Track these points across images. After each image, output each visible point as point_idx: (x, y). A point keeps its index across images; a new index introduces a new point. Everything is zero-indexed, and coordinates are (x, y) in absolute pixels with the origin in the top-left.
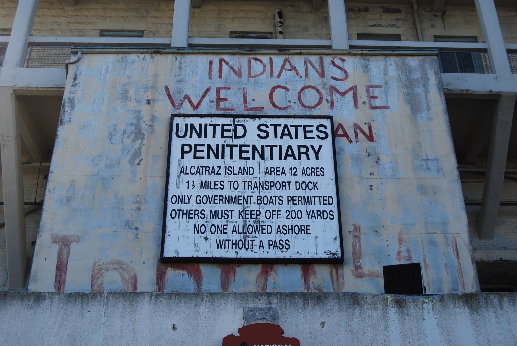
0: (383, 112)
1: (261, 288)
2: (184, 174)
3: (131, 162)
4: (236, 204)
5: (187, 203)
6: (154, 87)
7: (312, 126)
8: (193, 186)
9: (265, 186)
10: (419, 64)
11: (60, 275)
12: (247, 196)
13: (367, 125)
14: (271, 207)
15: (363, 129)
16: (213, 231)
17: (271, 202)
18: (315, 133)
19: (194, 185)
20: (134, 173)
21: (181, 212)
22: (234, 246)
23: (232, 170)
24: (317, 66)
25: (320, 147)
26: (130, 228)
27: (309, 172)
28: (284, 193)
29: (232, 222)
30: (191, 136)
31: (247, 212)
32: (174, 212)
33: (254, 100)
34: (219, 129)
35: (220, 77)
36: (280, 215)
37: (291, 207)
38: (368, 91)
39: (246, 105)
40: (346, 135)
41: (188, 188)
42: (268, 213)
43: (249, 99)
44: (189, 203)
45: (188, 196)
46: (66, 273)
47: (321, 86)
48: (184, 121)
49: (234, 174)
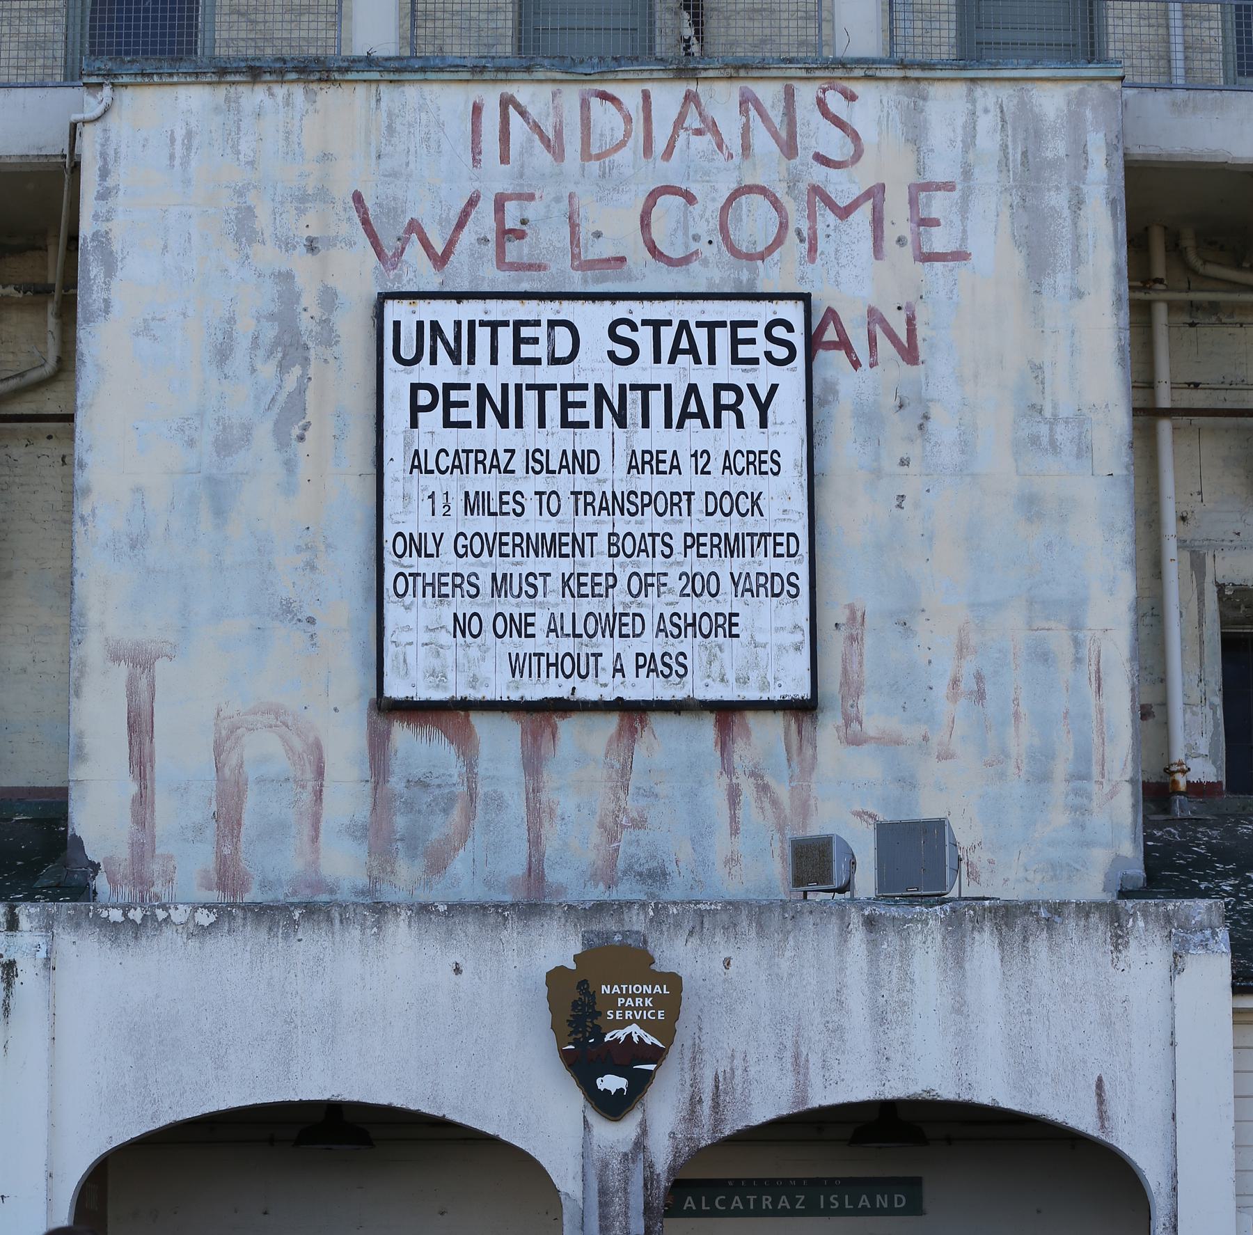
0: (950, 270)
1: (617, 771)
2: (421, 473)
4: (555, 556)
5: (432, 556)
6: (323, 194)
7: (753, 324)
8: (447, 508)
9: (627, 505)
10: (1065, 108)
11: (140, 743)
12: (583, 534)
13: (902, 311)
16: (500, 632)
17: (643, 551)
18: (763, 345)
19: (447, 505)
20: (290, 466)
21: (420, 579)
22: (553, 669)
23: (543, 459)
24: (776, 116)
25: (774, 388)
26: (296, 619)
27: (741, 462)
28: (678, 527)
30: (433, 361)
31: (583, 579)
32: (401, 579)
33: (598, 235)
34: (505, 335)
35: (505, 159)
36: (665, 585)
37: (693, 564)
38: (913, 202)
40: (844, 344)
41: (433, 514)
42: (635, 579)
43: (585, 232)
44: (438, 556)
45: (433, 534)
48: (414, 312)
49: (548, 472)
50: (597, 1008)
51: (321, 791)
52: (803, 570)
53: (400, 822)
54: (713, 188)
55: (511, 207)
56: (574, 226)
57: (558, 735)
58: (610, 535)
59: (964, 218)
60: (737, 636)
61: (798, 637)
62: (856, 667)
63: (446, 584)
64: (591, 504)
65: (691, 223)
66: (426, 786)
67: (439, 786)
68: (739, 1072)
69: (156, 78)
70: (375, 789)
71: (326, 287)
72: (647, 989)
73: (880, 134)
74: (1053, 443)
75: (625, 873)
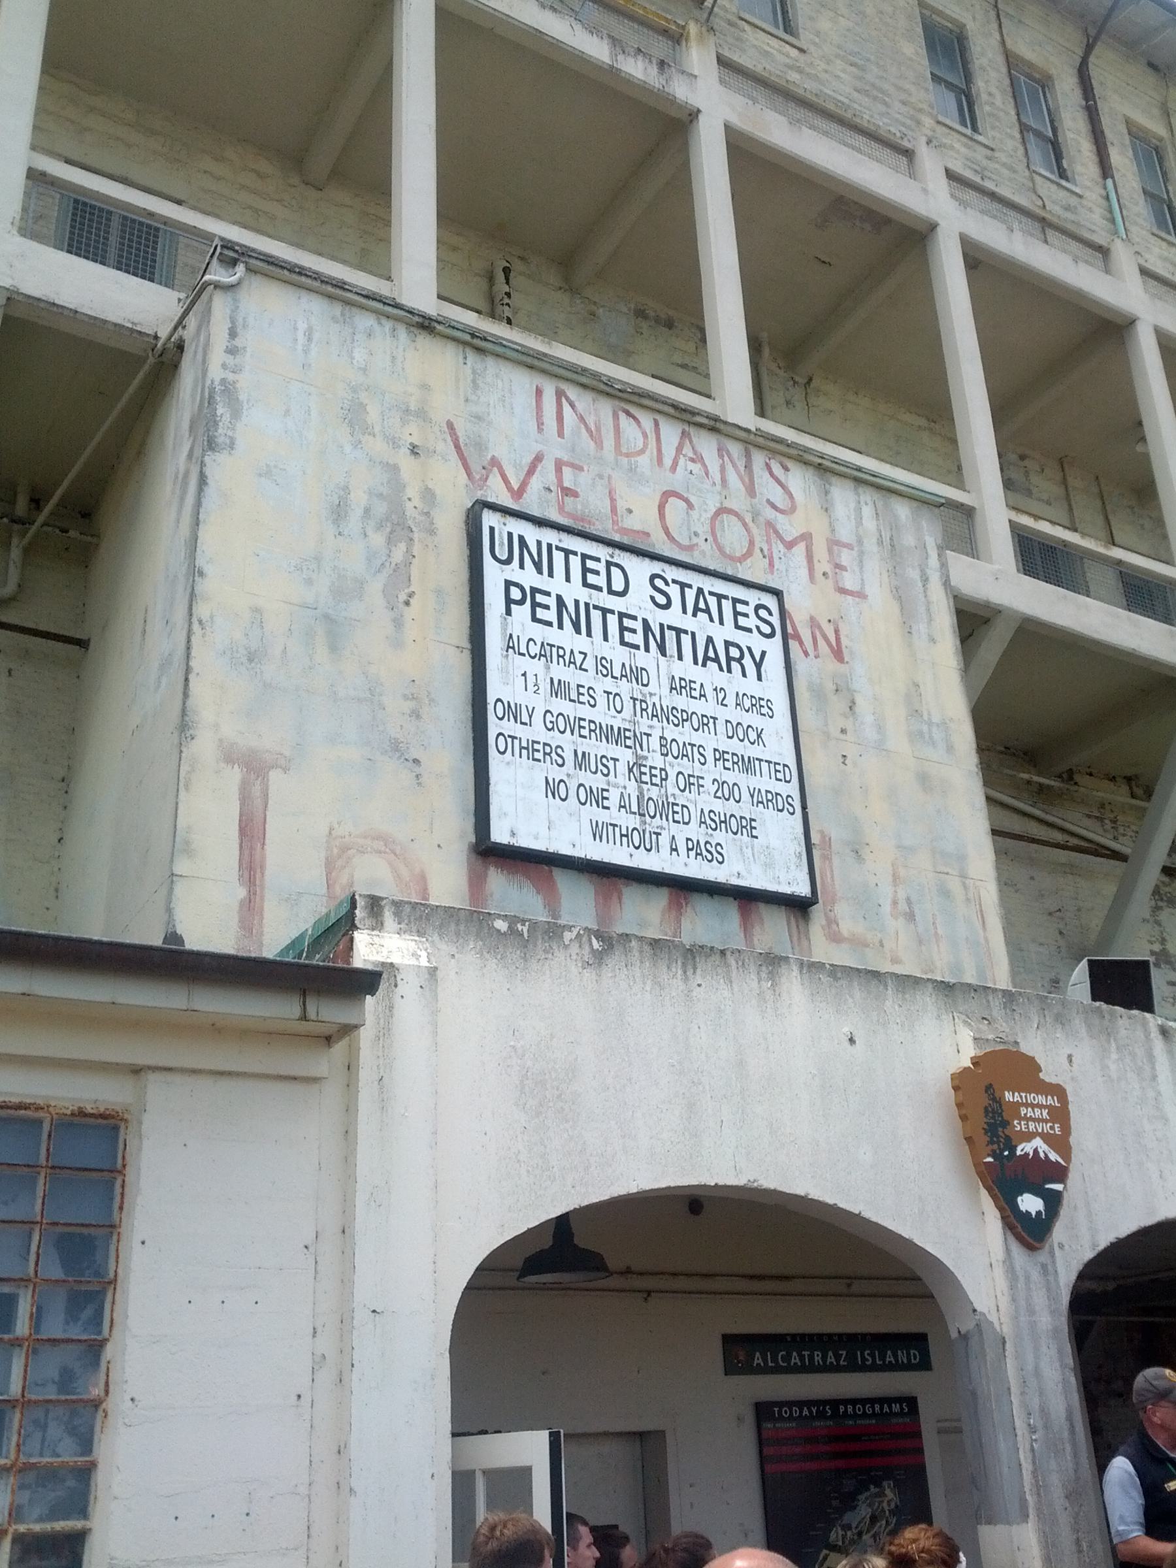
6: (422, 414)
9: (671, 717)
18: (752, 622)
20: (398, 623)
21: (516, 742)
23: (608, 666)
24: (741, 464)
25: (763, 654)
28: (710, 741)
29: (616, 786)
30: (522, 566)
31: (643, 769)
35: (561, 434)
38: (830, 551)
40: (797, 637)
46: (264, 844)
49: (612, 677)
52: (796, 795)
55: (567, 471)
63: (538, 751)
71: (427, 488)
72: (1041, 1099)
74: (931, 737)
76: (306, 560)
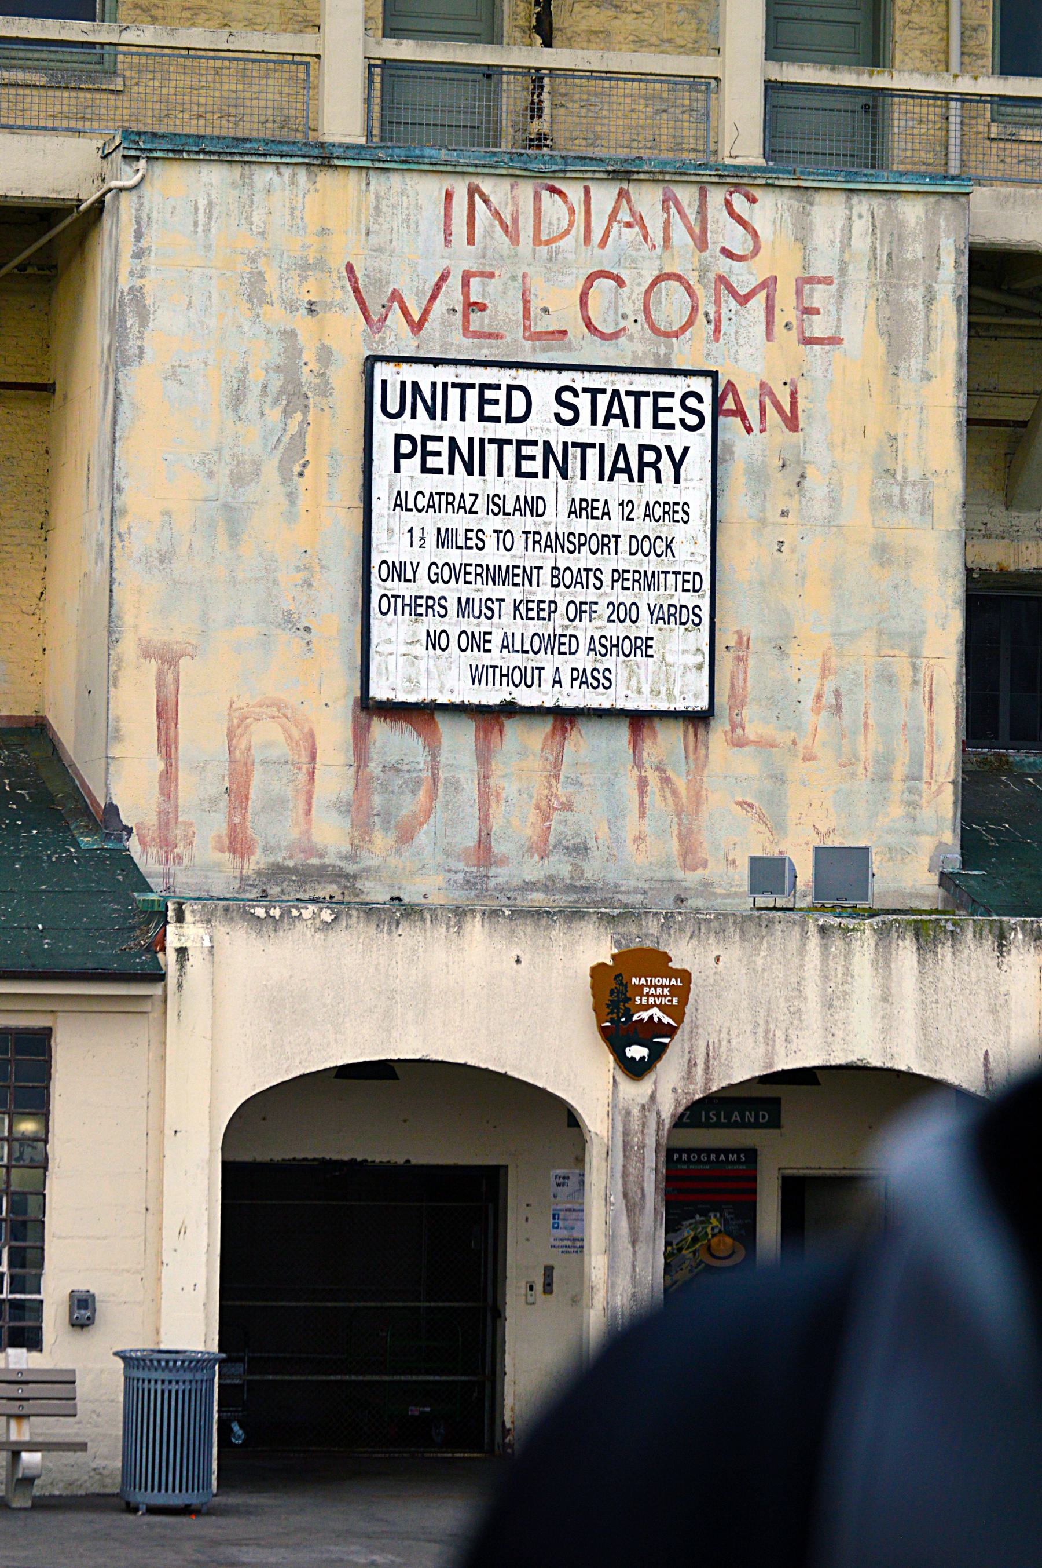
3: (284, 468)
5: (409, 581)
6: (321, 264)
7: (671, 395)
9: (567, 544)
10: (923, 216)
13: (787, 386)
14: (579, 594)
15: (779, 397)
16: (464, 647)
18: (679, 413)
20: (292, 497)
21: (399, 600)
22: (505, 679)
23: (501, 503)
24: (691, 214)
25: (686, 450)
27: (658, 512)
28: (607, 562)
30: (414, 416)
31: (530, 605)
32: (385, 600)
35: (471, 241)
36: (595, 612)
38: (799, 292)
39: (527, 323)
40: (740, 412)
42: (572, 607)
46: (176, 724)
47: (697, 273)
48: (398, 373)
49: (505, 514)
50: (628, 995)
51: (314, 772)
53: (377, 800)
54: (640, 275)
55: (474, 282)
56: (526, 302)
57: (504, 732)
58: (553, 568)
59: (839, 309)
60: (651, 656)
61: (699, 659)
62: (741, 683)
63: (421, 605)
64: (538, 542)
65: (620, 303)
66: (399, 771)
67: (409, 771)
68: (724, 1043)
69: (185, 155)
70: (357, 772)
72: (665, 981)
73: (774, 233)
74: (902, 501)
75: (555, 847)
76: (208, 454)
